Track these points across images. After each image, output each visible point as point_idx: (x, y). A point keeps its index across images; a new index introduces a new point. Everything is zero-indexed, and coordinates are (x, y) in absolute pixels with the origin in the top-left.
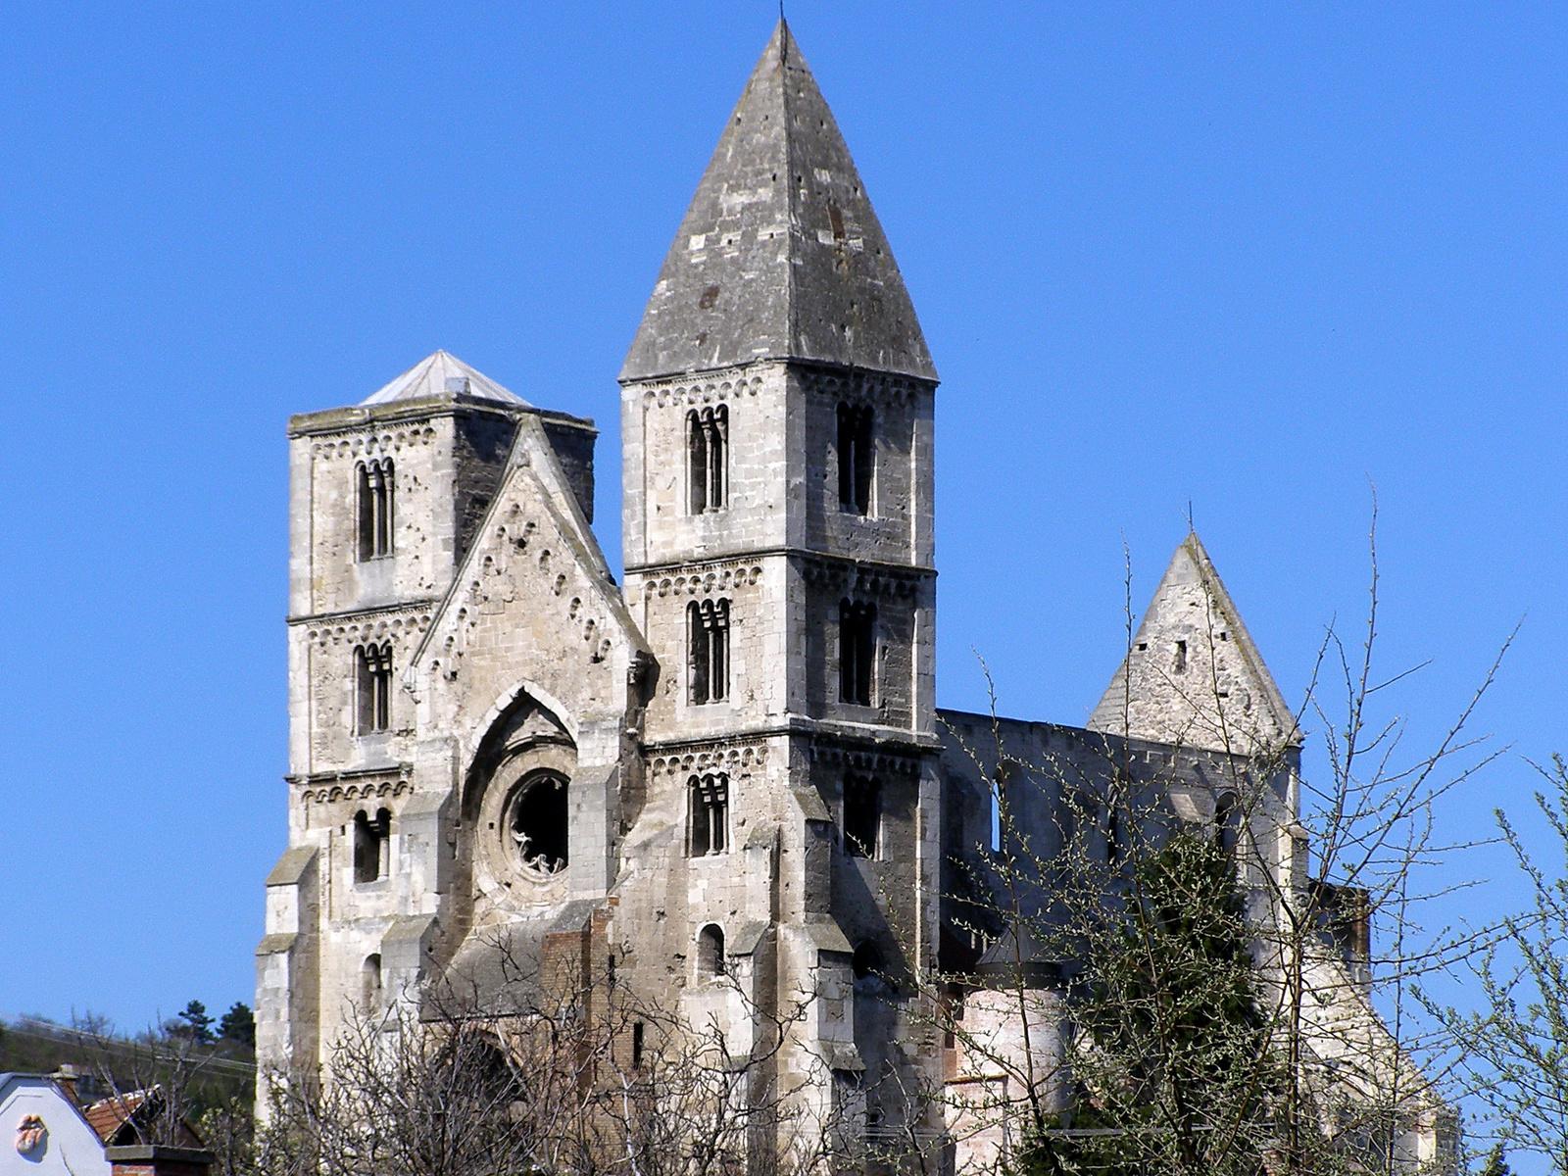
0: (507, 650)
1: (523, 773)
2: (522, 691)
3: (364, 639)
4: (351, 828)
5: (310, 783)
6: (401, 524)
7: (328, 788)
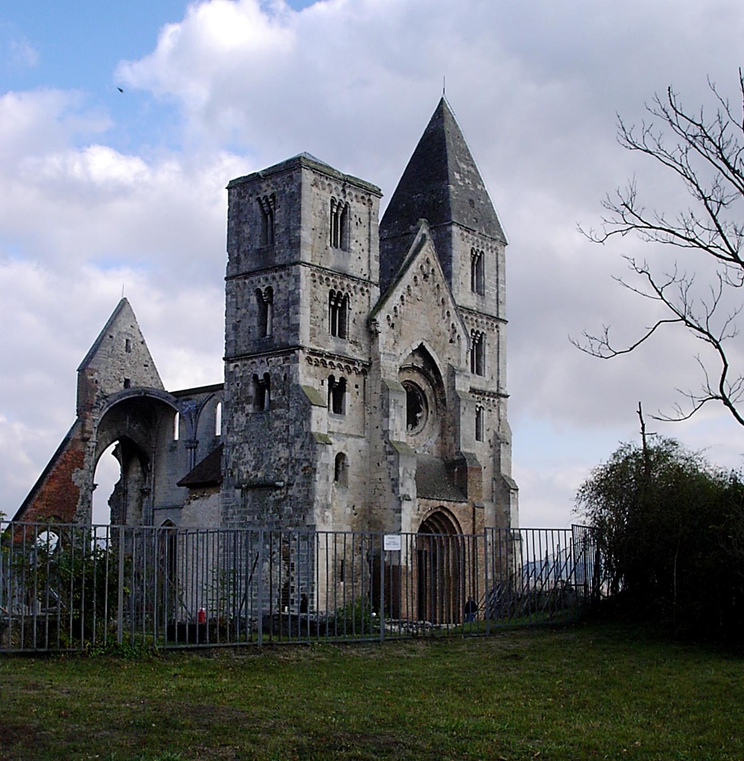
0: (417, 323)
1: (413, 380)
2: (422, 343)
3: (335, 287)
4: (326, 382)
5: (310, 353)
6: (354, 238)
7: (319, 359)
